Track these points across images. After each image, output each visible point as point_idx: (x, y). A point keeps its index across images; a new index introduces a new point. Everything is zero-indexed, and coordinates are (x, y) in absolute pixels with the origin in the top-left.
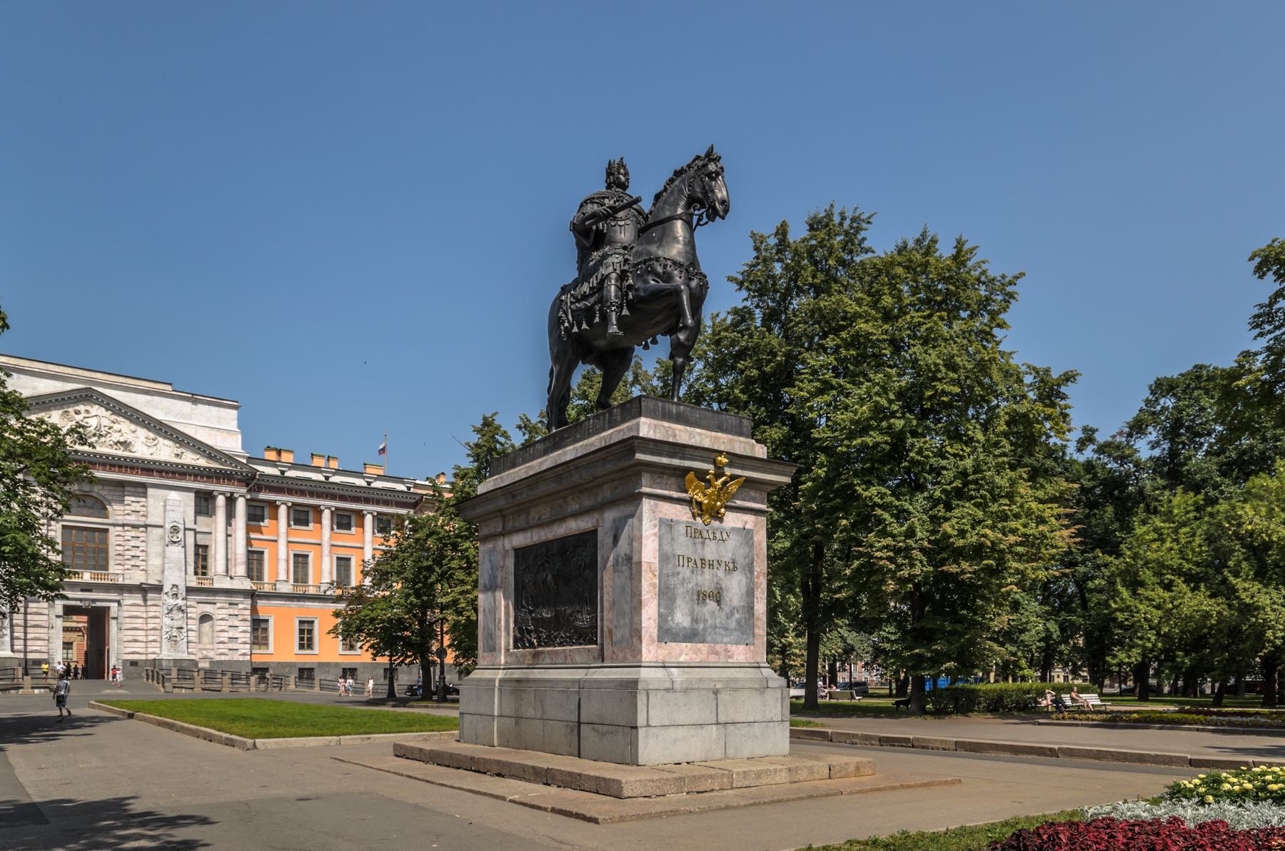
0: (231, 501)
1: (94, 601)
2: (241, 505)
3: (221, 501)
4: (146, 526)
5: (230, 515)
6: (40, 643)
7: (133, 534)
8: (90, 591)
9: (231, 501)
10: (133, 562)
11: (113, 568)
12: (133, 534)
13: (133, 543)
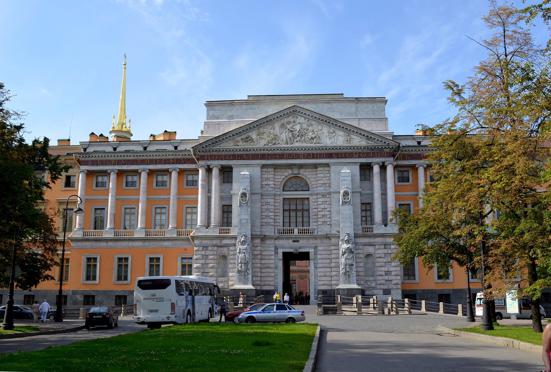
0: (383, 168)
1: (300, 248)
2: (390, 170)
3: (376, 169)
4: (330, 193)
5: (384, 180)
6: (270, 279)
8: (298, 241)
9: (383, 168)
11: (313, 226)
12: (323, 200)
13: (323, 206)
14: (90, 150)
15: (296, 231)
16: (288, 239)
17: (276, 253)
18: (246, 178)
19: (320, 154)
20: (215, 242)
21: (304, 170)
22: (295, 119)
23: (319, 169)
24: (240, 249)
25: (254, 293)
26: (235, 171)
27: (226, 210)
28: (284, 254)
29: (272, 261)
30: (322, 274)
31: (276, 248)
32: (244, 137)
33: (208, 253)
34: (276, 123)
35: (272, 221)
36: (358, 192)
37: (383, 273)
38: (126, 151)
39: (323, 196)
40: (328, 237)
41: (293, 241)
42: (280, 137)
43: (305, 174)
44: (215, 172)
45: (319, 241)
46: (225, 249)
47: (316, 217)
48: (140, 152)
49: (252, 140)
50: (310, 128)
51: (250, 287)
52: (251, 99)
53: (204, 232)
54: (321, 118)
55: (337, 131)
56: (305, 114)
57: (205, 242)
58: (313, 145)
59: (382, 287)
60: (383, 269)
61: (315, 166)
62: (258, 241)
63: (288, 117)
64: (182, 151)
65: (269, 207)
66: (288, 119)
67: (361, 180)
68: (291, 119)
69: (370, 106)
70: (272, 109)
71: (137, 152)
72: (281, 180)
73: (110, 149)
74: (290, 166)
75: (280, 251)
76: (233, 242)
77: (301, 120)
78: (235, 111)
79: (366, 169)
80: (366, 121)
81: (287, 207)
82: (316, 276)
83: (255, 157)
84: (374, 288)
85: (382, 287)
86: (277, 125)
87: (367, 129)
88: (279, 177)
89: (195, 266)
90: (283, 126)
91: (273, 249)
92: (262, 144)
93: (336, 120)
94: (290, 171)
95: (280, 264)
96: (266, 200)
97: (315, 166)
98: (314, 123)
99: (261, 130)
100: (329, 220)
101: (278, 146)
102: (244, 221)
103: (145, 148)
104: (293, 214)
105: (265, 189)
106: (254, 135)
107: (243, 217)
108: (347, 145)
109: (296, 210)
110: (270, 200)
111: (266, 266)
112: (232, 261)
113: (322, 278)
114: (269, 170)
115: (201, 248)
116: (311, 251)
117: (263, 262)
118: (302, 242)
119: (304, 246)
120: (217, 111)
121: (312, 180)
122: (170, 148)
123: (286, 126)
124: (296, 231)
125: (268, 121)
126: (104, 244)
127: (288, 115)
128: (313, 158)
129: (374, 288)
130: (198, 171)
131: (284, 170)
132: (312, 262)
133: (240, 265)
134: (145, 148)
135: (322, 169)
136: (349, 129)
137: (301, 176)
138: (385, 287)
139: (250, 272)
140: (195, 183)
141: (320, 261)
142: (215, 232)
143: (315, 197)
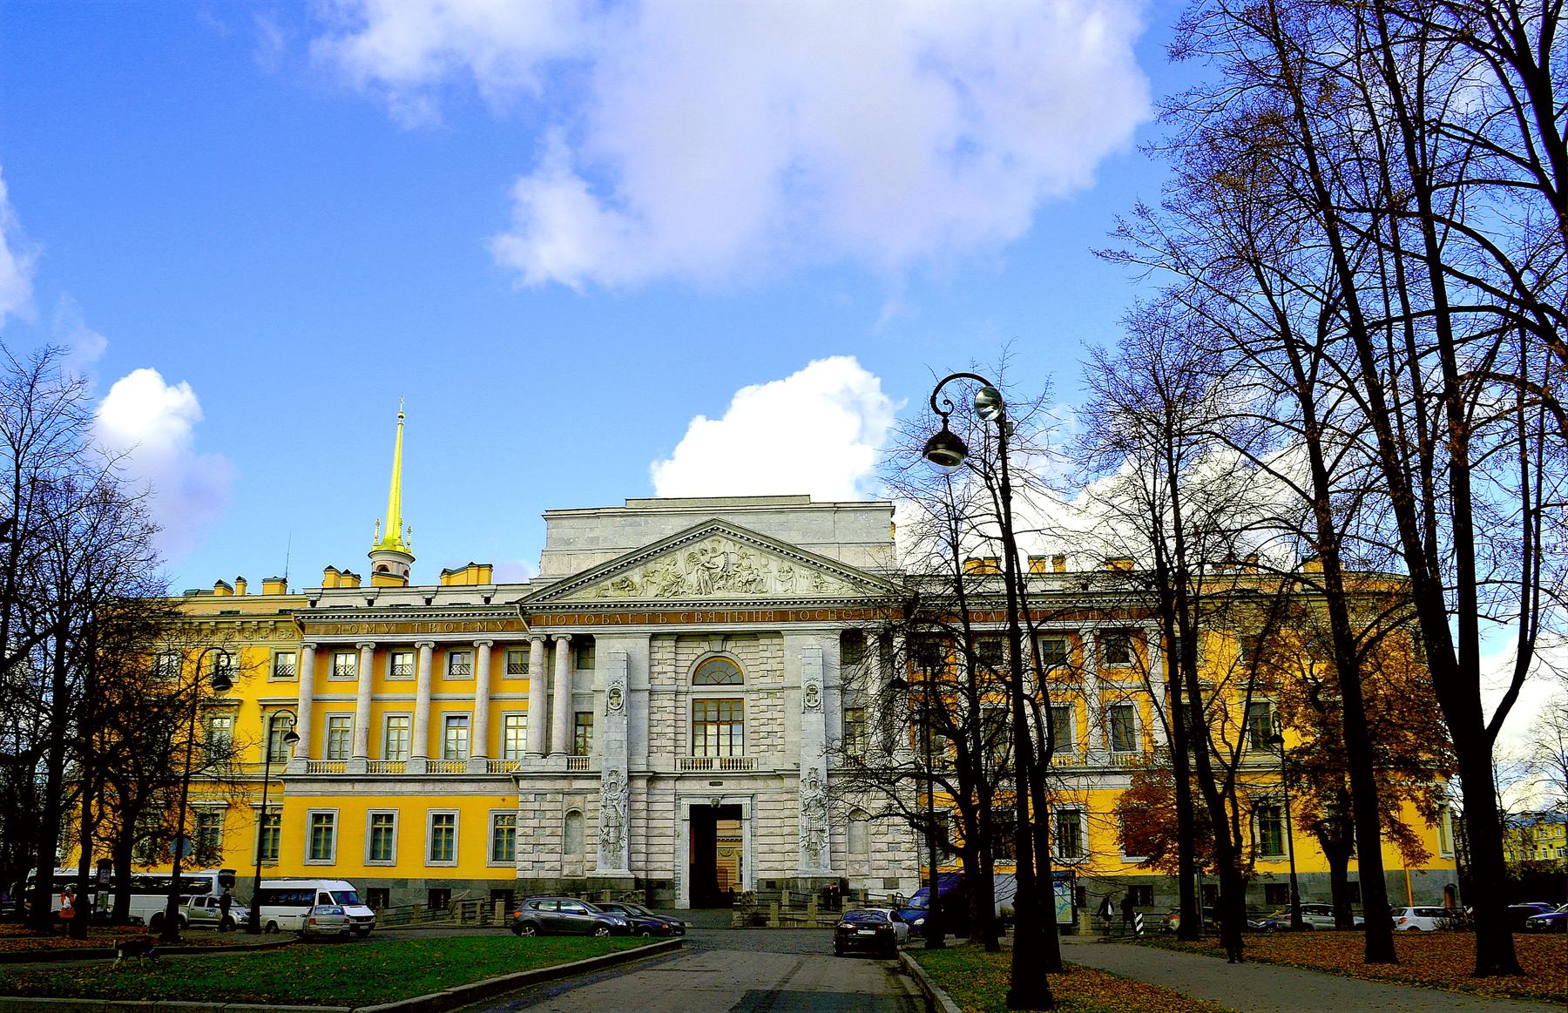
6: (665, 857)
7: (769, 702)
10: (768, 741)
12: (769, 702)
14: (323, 603)
15: (716, 764)
16: (701, 778)
17: (677, 807)
20: (561, 784)
22: (715, 545)
23: (762, 641)
25: (632, 884)
26: (600, 645)
27: (580, 720)
28: (692, 807)
29: (670, 823)
30: (766, 848)
31: (678, 797)
32: (617, 579)
33: (546, 806)
36: (836, 687)
37: (884, 846)
38: (394, 608)
39: (770, 692)
40: (777, 776)
42: (682, 578)
44: (562, 648)
45: (760, 784)
46: (578, 798)
47: (755, 736)
48: (419, 609)
49: (632, 586)
50: (745, 563)
51: (624, 872)
52: (631, 504)
53: (538, 765)
55: (796, 568)
57: (540, 784)
58: (748, 596)
59: (881, 873)
60: (885, 839)
61: (754, 635)
62: (641, 784)
64: (498, 607)
65: (666, 716)
66: (702, 545)
67: (844, 663)
68: (707, 544)
69: (862, 518)
70: (672, 526)
71: (413, 609)
73: (362, 603)
74: (704, 636)
75: (686, 804)
76: (593, 784)
77: (726, 546)
78: (602, 528)
79: (851, 642)
80: (853, 547)
81: (700, 716)
82: (754, 852)
83: (638, 618)
84: (865, 876)
85: (881, 873)
86: (681, 556)
87: (855, 565)
89: (519, 831)
92: (650, 594)
93: (793, 547)
94: (706, 646)
95: (685, 828)
96: (658, 703)
97: (754, 635)
98: (752, 551)
99: (651, 566)
100: (781, 741)
101: (682, 597)
102: (614, 745)
103: (428, 601)
104: (712, 729)
105: (656, 682)
106: (635, 576)
107: (613, 736)
108: (814, 594)
109: (718, 722)
110: (666, 703)
111: (656, 832)
112: (591, 822)
113: (767, 857)
114: (666, 643)
115: (532, 798)
116: (745, 802)
117: (653, 823)
118: (728, 786)
119: (732, 791)
120: (567, 528)
122: (477, 600)
124: (716, 764)
125: (664, 548)
126: (347, 787)
127: (703, 537)
128: (750, 621)
129: (865, 876)
130: (528, 644)
131: (695, 644)
132: (746, 825)
134: (428, 601)
135: (767, 641)
136: (819, 565)
138: (887, 874)
139: (625, 843)
140: (524, 668)
141: (763, 823)
142: (557, 764)
143: (754, 696)
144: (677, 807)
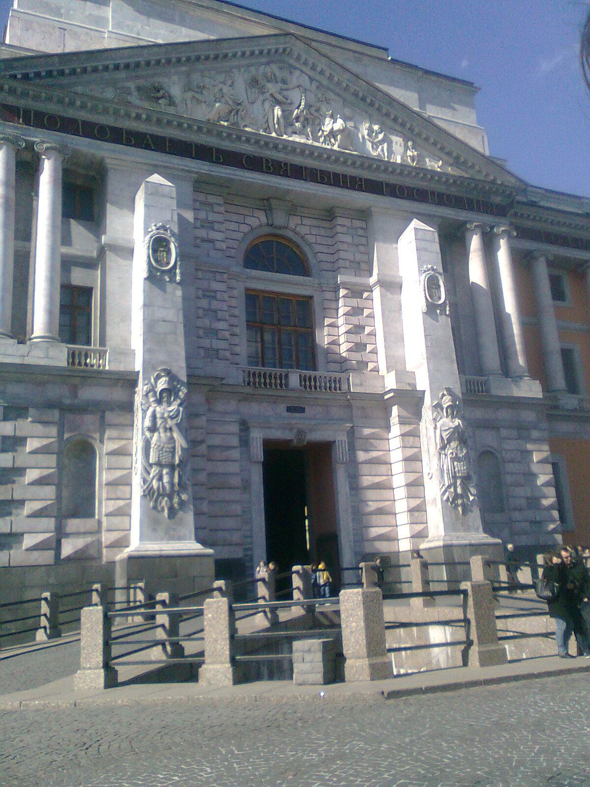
6: (230, 523)
8: (302, 410)
17: (245, 442)
18: (164, 196)
19: (353, 179)
21: (297, 220)
22: (285, 74)
23: (340, 221)
24: (154, 416)
29: (234, 467)
31: (245, 427)
34: (235, 71)
35: (222, 345)
37: (523, 502)
41: (289, 409)
43: (303, 230)
54: (353, 88)
56: (313, 68)
63: (268, 64)
65: (215, 305)
66: (268, 70)
72: (239, 236)
75: (257, 436)
88: (233, 226)
90: (254, 83)
91: (235, 428)
95: (257, 476)
98: (331, 95)
107: (161, 313)
110: (216, 286)
114: (211, 199)
116: (341, 438)
121: (317, 248)
123: (263, 87)
133: (154, 471)
135: (347, 222)
137: (290, 234)
144: (245, 442)
